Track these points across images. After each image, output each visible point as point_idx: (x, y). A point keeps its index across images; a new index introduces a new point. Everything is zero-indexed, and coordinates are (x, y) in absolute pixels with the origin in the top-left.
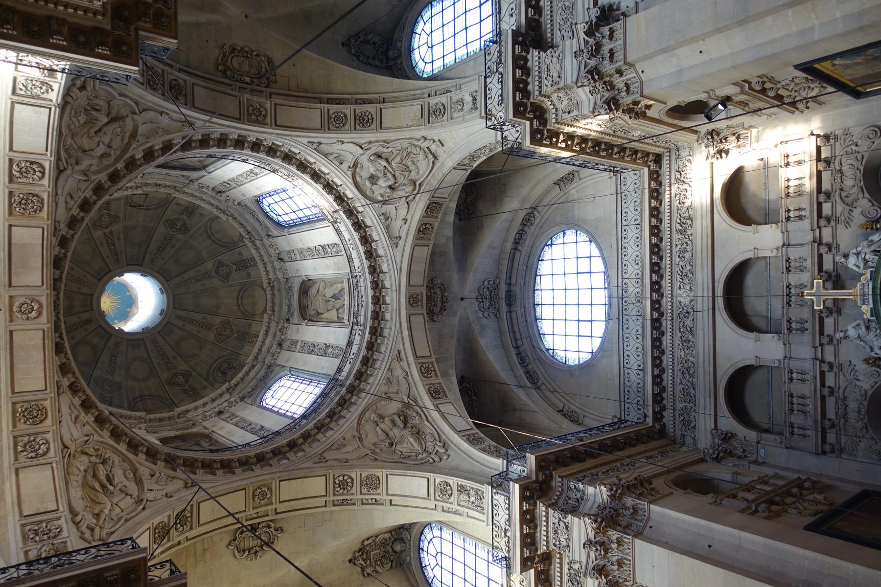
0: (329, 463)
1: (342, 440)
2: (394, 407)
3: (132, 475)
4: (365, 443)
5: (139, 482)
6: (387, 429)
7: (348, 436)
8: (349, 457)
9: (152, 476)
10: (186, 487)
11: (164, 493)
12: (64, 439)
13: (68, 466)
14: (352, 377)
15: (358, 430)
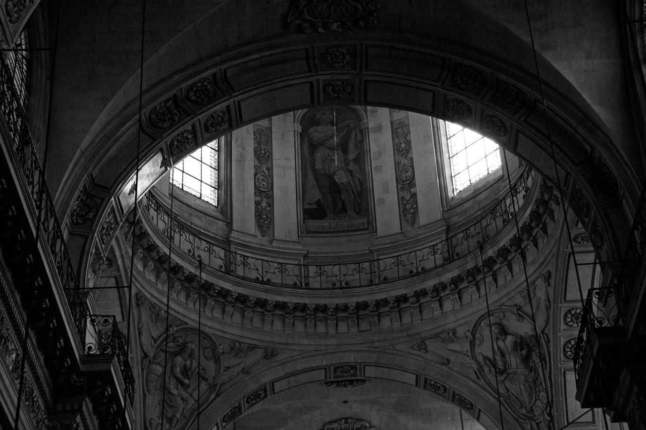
0: (428, 356)
1: (451, 334)
2: (524, 328)
3: (211, 353)
4: (477, 350)
5: (217, 360)
6: (505, 351)
7: (460, 332)
8: (452, 359)
9: (233, 349)
10: (265, 357)
11: (238, 369)
12: (144, 347)
13: (148, 373)
14: (496, 248)
15: (474, 336)
